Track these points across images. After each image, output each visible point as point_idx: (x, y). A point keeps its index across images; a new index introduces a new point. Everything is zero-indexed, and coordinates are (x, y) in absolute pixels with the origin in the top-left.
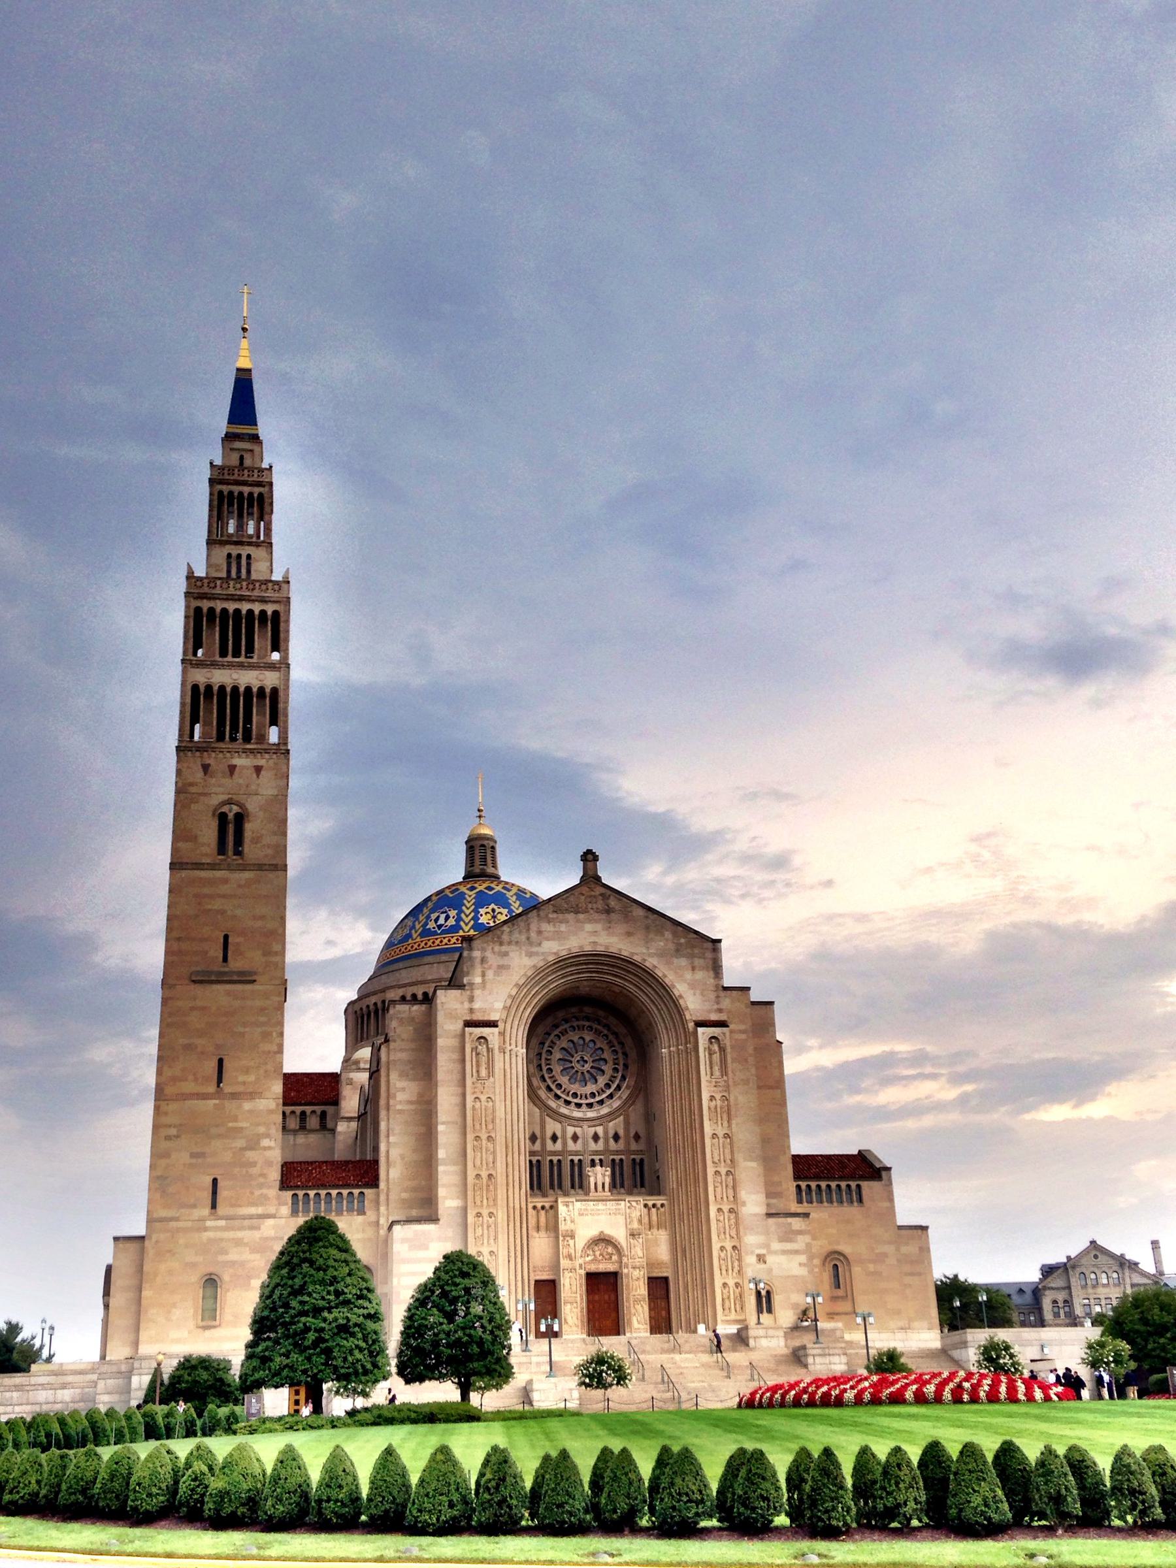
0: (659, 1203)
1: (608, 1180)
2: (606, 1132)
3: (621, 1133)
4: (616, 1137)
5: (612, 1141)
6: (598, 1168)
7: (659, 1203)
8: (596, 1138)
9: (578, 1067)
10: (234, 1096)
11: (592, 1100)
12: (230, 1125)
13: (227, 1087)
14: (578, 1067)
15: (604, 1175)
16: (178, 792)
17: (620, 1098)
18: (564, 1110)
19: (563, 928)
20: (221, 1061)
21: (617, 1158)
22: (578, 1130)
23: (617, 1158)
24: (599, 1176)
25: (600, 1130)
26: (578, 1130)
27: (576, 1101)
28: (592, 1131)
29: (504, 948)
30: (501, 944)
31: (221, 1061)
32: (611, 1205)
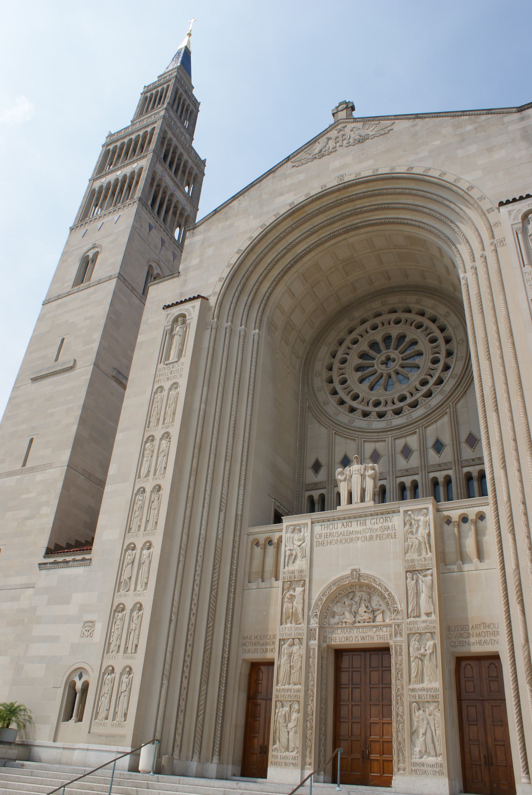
0: (472, 513)
1: (369, 484)
2: (423, 441)
3: (446, 439)
4: (438, 446)
5: (432, 453)
6: (355, 467)
7: (472, 513)
8: (407, 452)
9: (381, 369)
10: (33, 469)
11: (402, 404)
12: (23, 497)
13: (28, 465)
14: (381, 369)
15: (363, 476)
16: (64, 254)
17: (441, 392)
18: (360, 423)
19: (302, 177)
20: (31, 440)
21: (440, 476)
22: (380, 446)
23: (440, 476)
24: (356, 479)
25: (413, 441)
26: (380, 446)
27: (378, 409)
28: (400, 443)
29: (228, 222)
30: (226, 219)
31: (31, 440)
32: (374, 524)
